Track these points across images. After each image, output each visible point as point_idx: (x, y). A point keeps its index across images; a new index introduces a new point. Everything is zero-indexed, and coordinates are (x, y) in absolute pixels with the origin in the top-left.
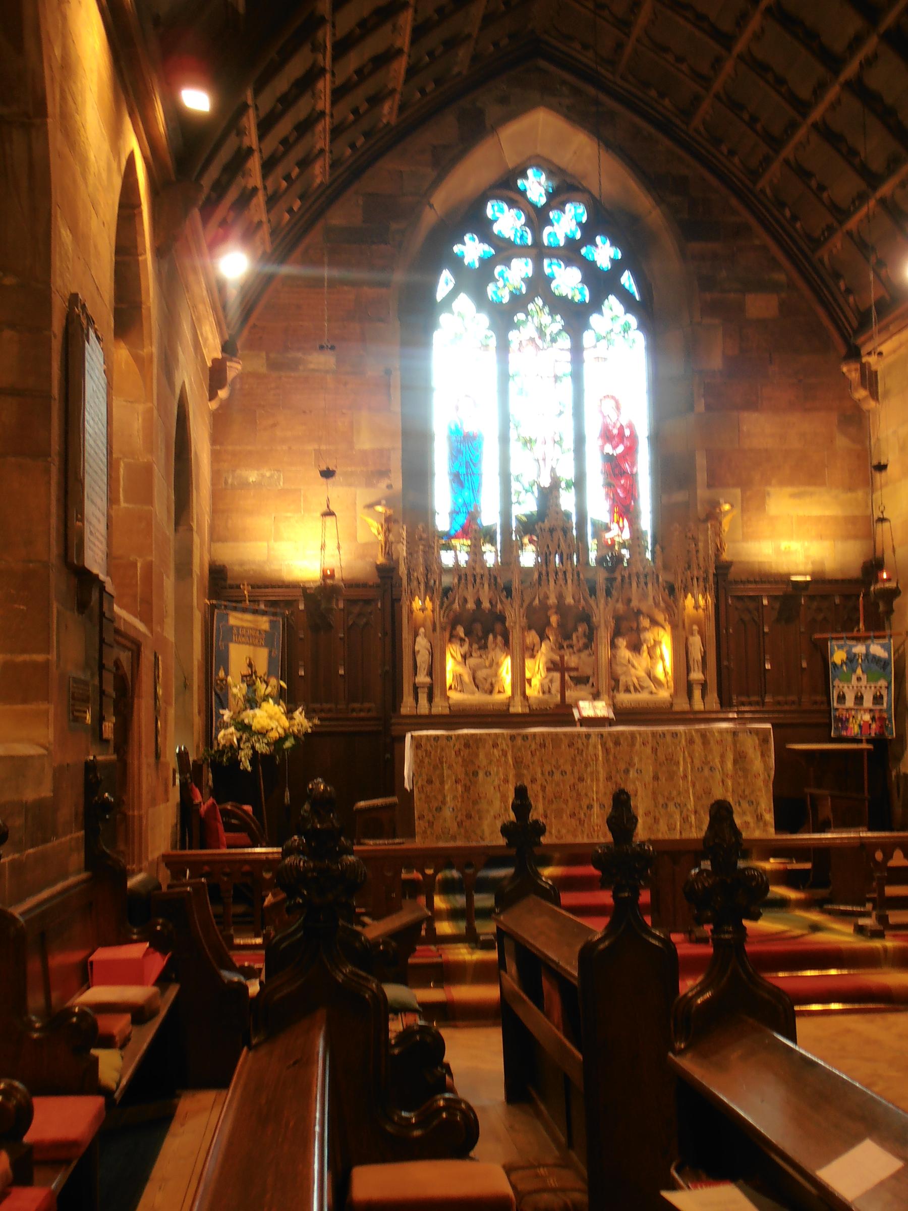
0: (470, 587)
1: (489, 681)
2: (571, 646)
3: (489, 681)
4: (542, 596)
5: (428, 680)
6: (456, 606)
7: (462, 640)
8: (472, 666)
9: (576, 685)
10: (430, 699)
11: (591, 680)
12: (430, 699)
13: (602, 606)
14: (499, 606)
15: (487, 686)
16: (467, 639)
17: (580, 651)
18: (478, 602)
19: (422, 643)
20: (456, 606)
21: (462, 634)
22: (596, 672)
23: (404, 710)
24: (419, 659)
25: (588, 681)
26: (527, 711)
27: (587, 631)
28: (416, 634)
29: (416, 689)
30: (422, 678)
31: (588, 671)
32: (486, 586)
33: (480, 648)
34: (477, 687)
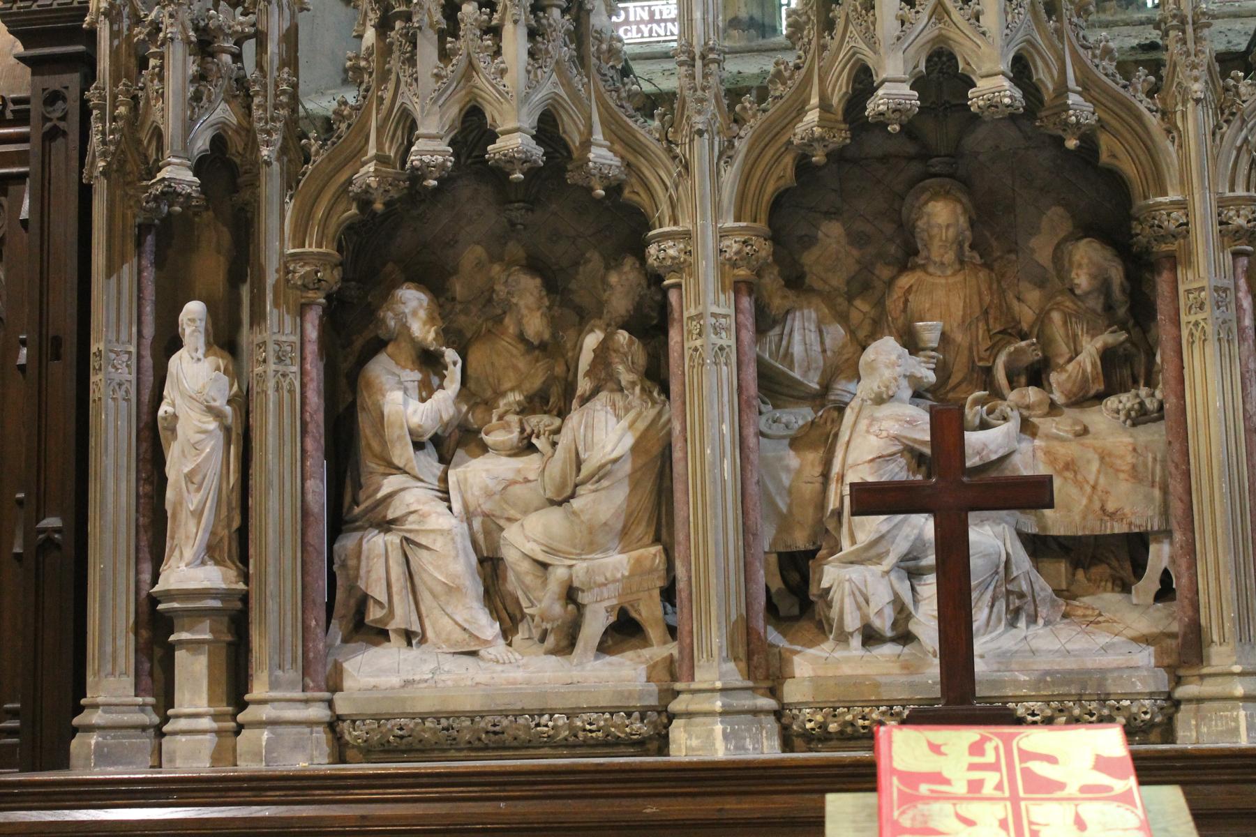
0: (428, 51)
1: (559, 573)
2: (1037, 375)
3: (559, 573)
4: (839, 91)
5: (213, 577)
6: (367, 173)
7: (429, 361)
8: (475, 495)
9: (1066, 594)
10: (235, 685)
11: (1160, 556)
12: (235, 685)
13: (1194, 122)
14: (602, 156)
15: (544, 603)
16: (450, 355)
17: (1084, 399)
18: (473, 130)
19: (195, 374)
20: (367, 173)
21: (422, 329)
22: (1180, 513)
23: (88, 760)
24: (177, 465)
25: (1139, 568)
26: (767, 748)
27: (1116, 274)
28: (169, 342)
29: (156, 627)
30: (189, 572)
31: (1133, 507)
32: (515, 43)
33: (536, 403)
34: (509, 617)
